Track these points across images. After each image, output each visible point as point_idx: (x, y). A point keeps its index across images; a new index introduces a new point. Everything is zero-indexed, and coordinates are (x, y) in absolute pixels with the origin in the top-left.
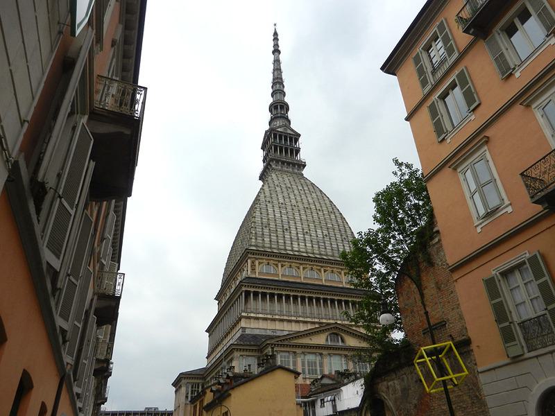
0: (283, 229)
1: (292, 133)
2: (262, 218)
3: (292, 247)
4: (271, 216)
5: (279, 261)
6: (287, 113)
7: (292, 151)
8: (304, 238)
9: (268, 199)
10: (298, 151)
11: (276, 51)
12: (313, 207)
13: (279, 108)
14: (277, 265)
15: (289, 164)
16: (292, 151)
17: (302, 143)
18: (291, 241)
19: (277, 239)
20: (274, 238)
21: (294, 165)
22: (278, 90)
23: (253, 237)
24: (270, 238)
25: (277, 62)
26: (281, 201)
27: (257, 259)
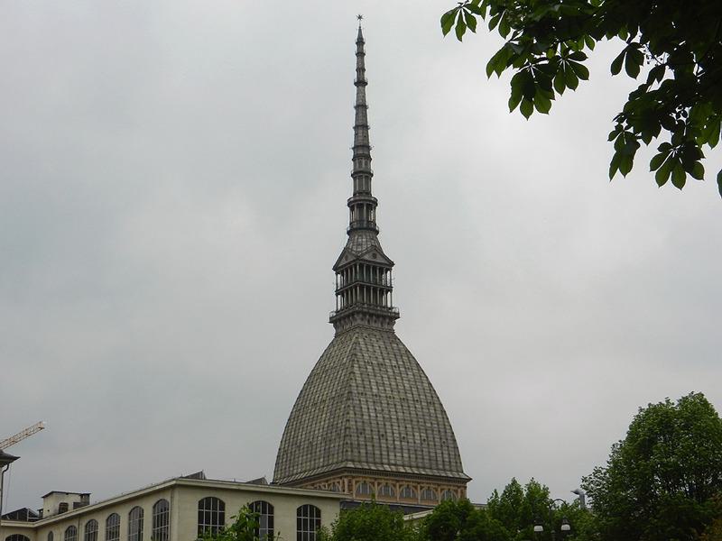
0: (379, 435)
1: (383, 261)
2: (356, 422)
4: (366, 417)
9: (361, 389)
10: (390, 289)
11: (361, 83)
13: (363, 204)
15: (378, 316)
17: (395, 277)
18: (388, 452)
19: (374, 450)
20: (370, 448)
21: (384, 317)
23: (349, 449)
24: (366, 449)
25: (361, 107)
26: (375, 391)
27: (353, 477)
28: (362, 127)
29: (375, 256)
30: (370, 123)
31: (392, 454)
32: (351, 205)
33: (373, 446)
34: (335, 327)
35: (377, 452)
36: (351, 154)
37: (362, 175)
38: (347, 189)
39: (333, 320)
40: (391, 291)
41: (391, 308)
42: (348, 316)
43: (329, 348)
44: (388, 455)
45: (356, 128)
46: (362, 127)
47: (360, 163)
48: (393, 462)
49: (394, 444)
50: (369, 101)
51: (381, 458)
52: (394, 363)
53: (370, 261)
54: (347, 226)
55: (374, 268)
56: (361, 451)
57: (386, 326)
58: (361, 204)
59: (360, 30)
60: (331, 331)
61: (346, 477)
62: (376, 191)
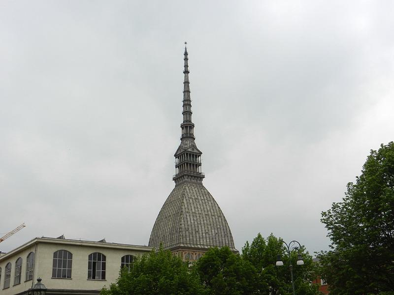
1: (197, 152)
3: (200, 243)
4: (189, 223)
5: (194, 252)
8: (206, 236)
9: (187, 210)
10: (200, 165)
11: (186, 72)
13: (188, 126)
14: (193, 254)
15: (195, 177)
17: (202, 159)
20: (191, 237)
21: (198, 177)
22: (188, 112)
25: (187, 83)
26: (193, 211)
27: (183, 251)
28: (187, 92)
29: (193, 149)
31: (201, 240)
32: (182, 127)
33: (193, 236)
35: (195, 239)
37: (187, 113)
38: (181, 120)
39: (175, 179)
40: (201, 165)
41: (201, 173)
42: (181, 177)
43: (173, 192)
44: (200, 240)
45: (184, 92)
46: (187, 92)
48: (202, 244)
50: (190, 80)
52: (202, 198)
54: (180, 136)
55: (193, 155)
58: (187, 126)
59: (186, 49)
60: (173, 184)
62: (194, 119)
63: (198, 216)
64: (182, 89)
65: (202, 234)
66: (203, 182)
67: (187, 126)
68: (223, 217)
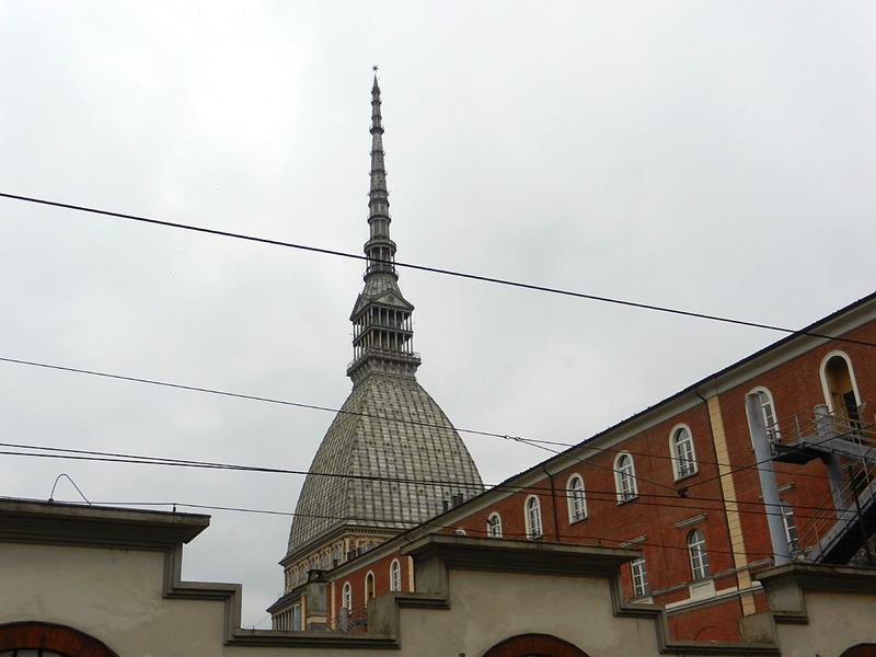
1: (402, 304)
3: (402, 516)
6: (393, 255)
7: (400, 336)
8: (418, 500)
9: (369, 438)
10: (409, 335)
11: (377, 130)
12: (430, 445)
13: (380, 253)
15: (395, 362)
16: (400, 336)
17: (416, 322)
18: (401, 507)
20: (378, 503)
21: (403, 363)
22: (379, 216)
23: (352, 505)
25: (378, 153)
26: (387, 439)
27: (357, 537)
28: (378, 172)
30: (387, 168)
31: (406, 510)
33: (382, 501)
34: (353, 380)
35: (388, 508)
36: (368, 199)
40: (411, 336)
44: (401, 511)
46: (378, 172)
47: (376, 208)
48: (407, 519)
49: (409, 499)
51: (392, 515)
52: (413, 410)
53: (386, 305)
55: (391, 313)
56: (367, 506)
57: (406, 373)
58: (378, 248)
60: (349, 384)
61: (346, 537)
62: (395, 233)
63: (398, 451)
64: (368, 168)
65: (409, 494)
66: (416, 374)
67: (378, 248)
68: (464, 455)
